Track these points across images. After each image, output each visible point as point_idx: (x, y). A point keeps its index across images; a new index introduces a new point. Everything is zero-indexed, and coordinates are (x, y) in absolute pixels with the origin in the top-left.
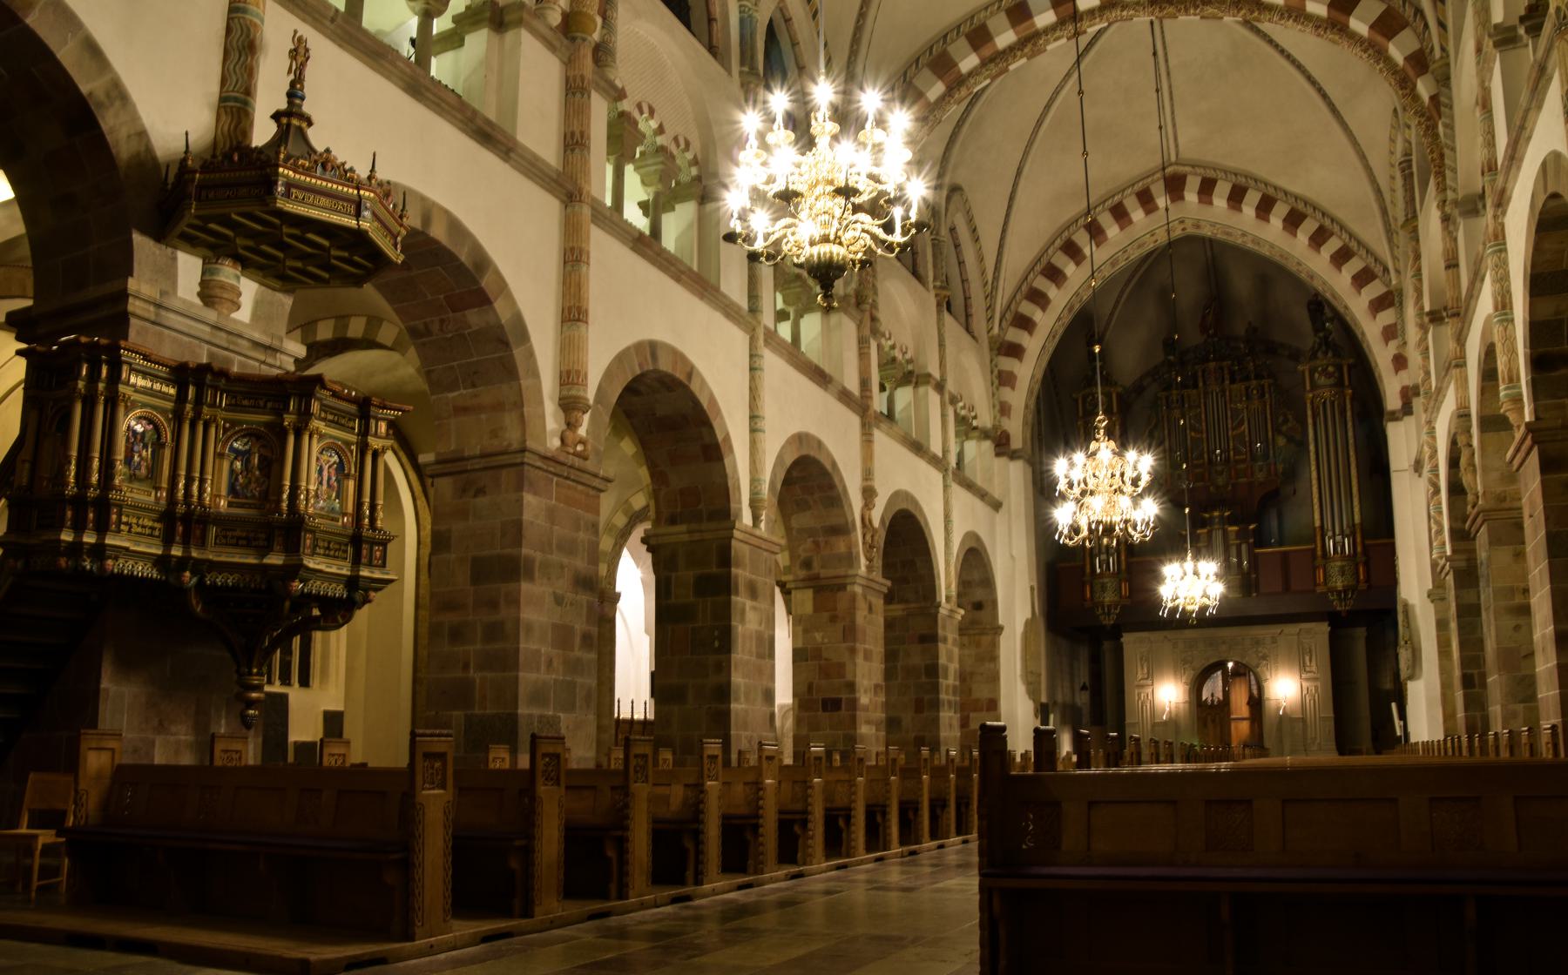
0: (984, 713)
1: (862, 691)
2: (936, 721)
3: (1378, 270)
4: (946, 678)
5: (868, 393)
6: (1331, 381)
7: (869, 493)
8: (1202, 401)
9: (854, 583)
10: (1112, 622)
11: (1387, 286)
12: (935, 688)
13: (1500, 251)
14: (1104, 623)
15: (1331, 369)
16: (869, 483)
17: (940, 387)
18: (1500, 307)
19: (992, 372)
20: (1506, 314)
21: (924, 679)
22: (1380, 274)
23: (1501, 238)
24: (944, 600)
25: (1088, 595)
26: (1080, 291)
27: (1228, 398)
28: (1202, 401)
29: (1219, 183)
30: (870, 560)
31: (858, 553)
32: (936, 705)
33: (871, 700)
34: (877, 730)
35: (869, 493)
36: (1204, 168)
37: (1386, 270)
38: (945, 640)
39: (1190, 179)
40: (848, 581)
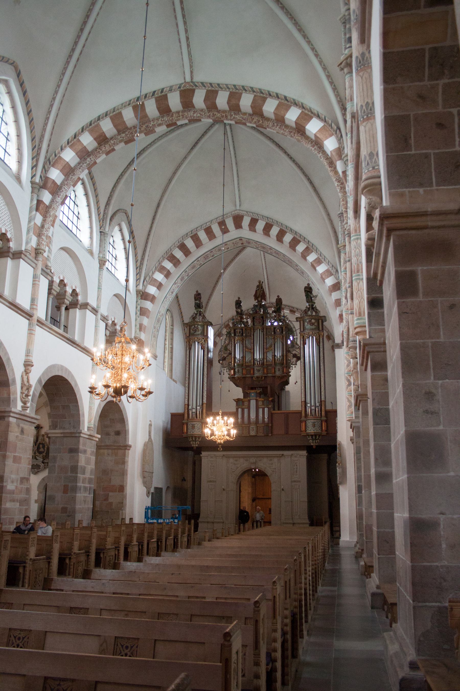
0: (117, 493)
1: (9, 481)
2: (74, 499)
3: (333, 271)
4: (84, 473)
5: (35, 307)
6: (313, 327)
7: (28, 365)
8: (252, 333)
9: (10, 416)
10: (197, 445)
11: (337, 279)
12: (75, 479)
13: (357, 239)
14: (193, 445)
15: (313, 321)
16: (29, 358)
17: (95, 311)
18: (356, 272)
19: (136, 308)
20: (359, 275)
21: (69, 474)
22: (334, 273)
23: (358, 232)
24: (86, 429)
25: (185, 431)
26: (187, 270)
27: (265, 333)
28: (252, 333)
29: (260, 221)
30: (25, 403)
31: (16, 399)
32: (75, 489)
33: (16, 487)
34: (20, 505)
35: (28, 365)
36: (252, 213)
37: (337, 271)
38: (85, 452)
39: (245, 218)
40: (6, 415)
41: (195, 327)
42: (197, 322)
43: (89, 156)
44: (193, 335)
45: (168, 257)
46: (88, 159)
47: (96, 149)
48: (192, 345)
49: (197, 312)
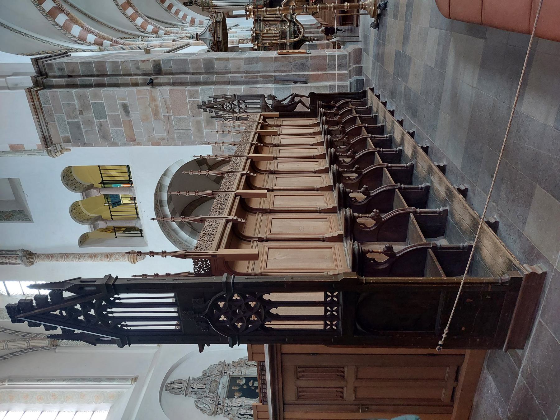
41: (204, 3)
42: (201, 2)
43: (137, 12)
44: (208, 4)
45: (169, 10)
46: (139, 12)
47: (134, 8)
48: (214, 5)
49: (194, 3)
